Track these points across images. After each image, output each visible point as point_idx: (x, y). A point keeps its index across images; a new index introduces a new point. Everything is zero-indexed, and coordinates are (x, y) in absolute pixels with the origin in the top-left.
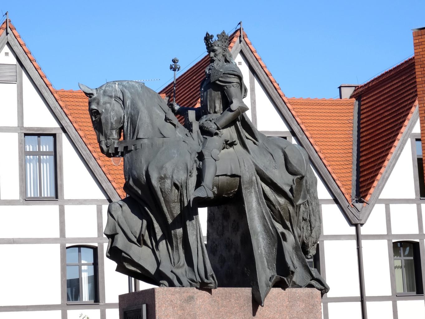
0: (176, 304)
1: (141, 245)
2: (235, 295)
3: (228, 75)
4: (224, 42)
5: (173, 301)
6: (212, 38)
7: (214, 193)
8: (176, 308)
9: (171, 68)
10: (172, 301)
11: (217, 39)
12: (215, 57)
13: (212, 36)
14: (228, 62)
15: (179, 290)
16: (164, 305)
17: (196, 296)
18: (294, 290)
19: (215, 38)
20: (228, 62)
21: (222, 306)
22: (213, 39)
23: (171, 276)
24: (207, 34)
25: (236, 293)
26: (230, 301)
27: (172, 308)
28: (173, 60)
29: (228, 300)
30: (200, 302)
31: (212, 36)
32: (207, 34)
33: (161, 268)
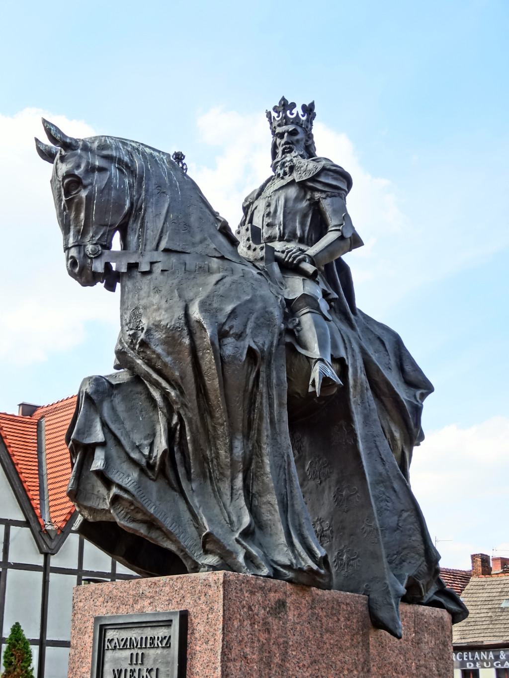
0: (257, 615)
2: (345, 607)
5: (253, 608)
8: (256, 627)
10: (250, 608)
11: (301, 113)
13: (293, 105)
15: (263, 584)
16: (238, 616)
17: (289, 600)
21: (327, 631)
22: (294, 111)
24: (283, 99)
26: (339, 620)
27: (251, 625)
29: (335, 618)
31: (293, 105)
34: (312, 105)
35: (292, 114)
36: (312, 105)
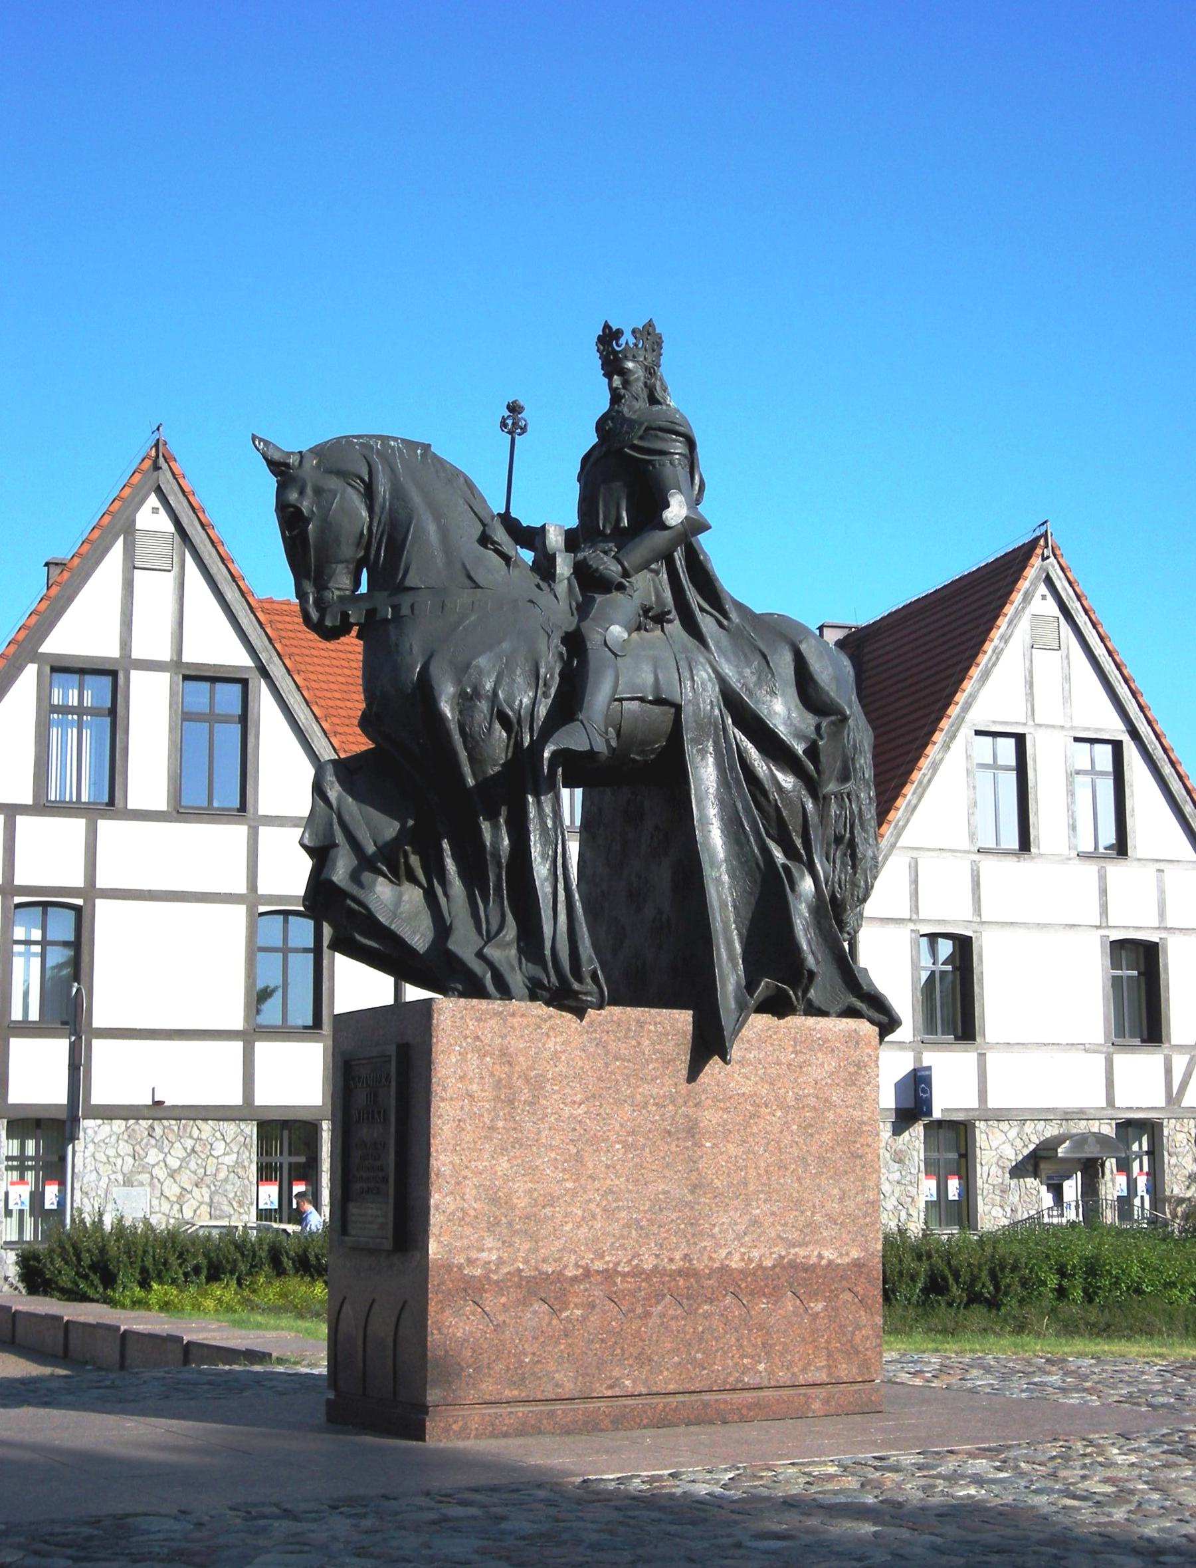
1: (398, 879)
2: (652, 1028)
3: (660, 434)
4: (650, 351)
5: (483, 1038)
6: (617, 339)
7: (607, 741)
9: (504, 424)
10: (477, 1038)
11: (632, 340)
12: (624, 388)
13: (619, 333)
14: (659, 403)
18: (811, 1021)
19: (627, 338)
20: (659, 403)
22: (622, 341)
23: (476, 966)
24: (607, 326)
25: (656, 1024)
26: (639, 1044)
28: (508, 407)
29: (634, 1042)
30: (556, 1043)
31: (619, 333)
32: (607, 326)
33: (452, 945)
34: (650, 324)
35: (618, 345)
36: (650, 324)
